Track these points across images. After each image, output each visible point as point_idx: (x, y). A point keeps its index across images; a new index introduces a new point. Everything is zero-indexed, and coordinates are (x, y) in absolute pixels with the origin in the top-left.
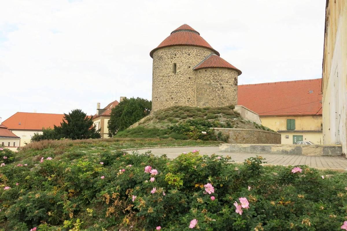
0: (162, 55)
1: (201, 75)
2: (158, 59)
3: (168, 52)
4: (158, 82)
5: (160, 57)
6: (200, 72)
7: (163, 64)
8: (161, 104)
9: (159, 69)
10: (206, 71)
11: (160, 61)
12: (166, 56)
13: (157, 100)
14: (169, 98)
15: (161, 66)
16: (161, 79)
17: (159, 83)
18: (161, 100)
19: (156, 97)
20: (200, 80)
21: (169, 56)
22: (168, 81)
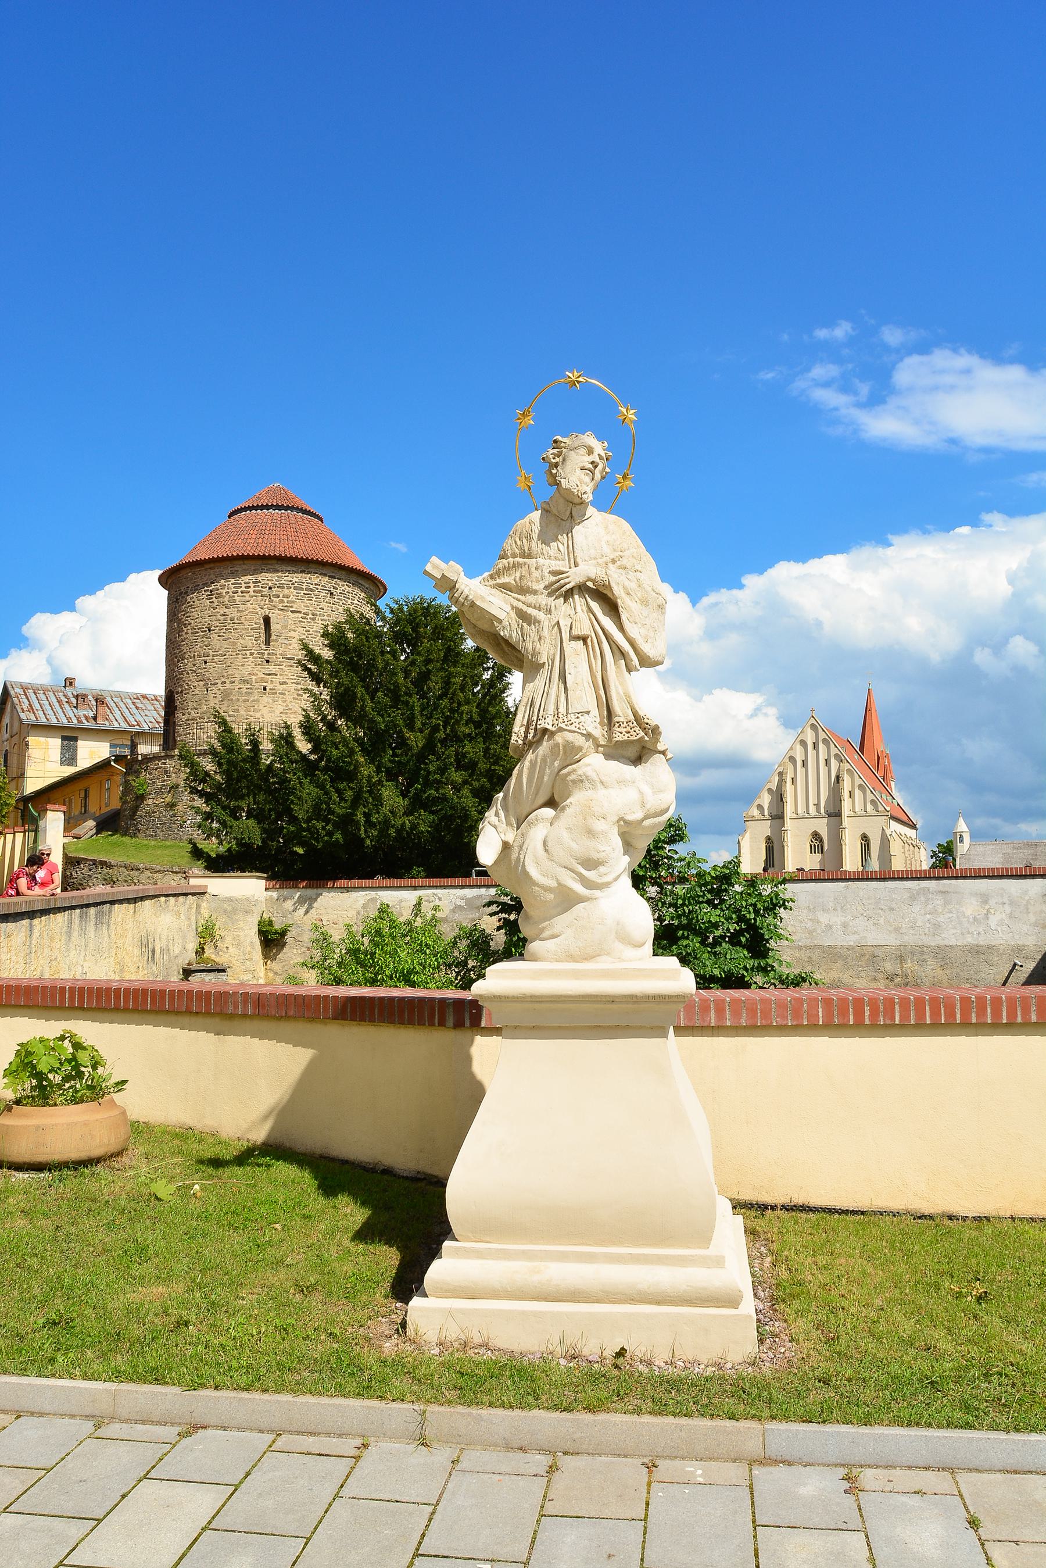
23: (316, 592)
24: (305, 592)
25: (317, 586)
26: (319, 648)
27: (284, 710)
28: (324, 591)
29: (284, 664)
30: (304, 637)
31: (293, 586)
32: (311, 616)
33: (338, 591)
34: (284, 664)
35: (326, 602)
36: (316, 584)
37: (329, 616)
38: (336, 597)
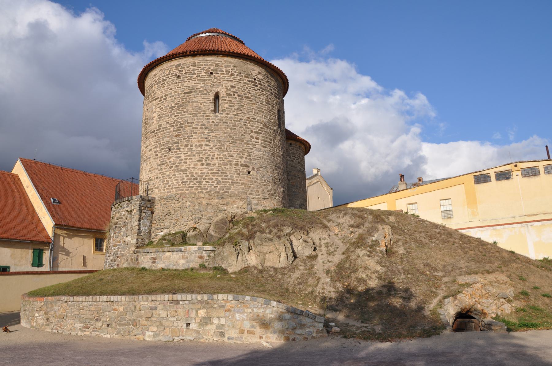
0: (260, 77)
1: (292, 151)
2: (248, 81)
3: (270, 79)
4: (252, 132)
5: (255, 79)
6: (291, 144)
7: (262, 97)
8: (265, 185)
9: (255, 104)
10: (299, 147)
11: (256, 88)
12: (268, 86)
13: (249, 172)
14: (277, 179)
15: (257, 100)
16: (259, 128)
17: (255, 135)
18: (263, 177)
19: (248, 166)
20: (292, 159)
21: (273, 90)
22: (274, 142)
23: (168, 80)
24: (162, 83)
25: (168, 76)
26: (168, 117)
27: (150, 168)
28: (172, 77)
29: (151, 137)
30: (160, 113)
31: (156, 83)
32: (164, 97)
33: (184, 72)
34: (151, 137)
35: (174, 84)
36: (167, 75)
37: (176, 92)
38: (181, 77)
